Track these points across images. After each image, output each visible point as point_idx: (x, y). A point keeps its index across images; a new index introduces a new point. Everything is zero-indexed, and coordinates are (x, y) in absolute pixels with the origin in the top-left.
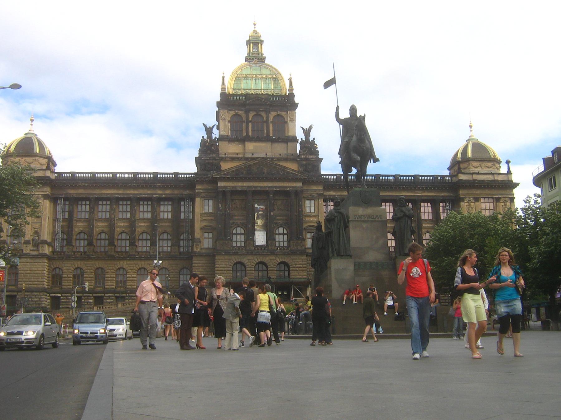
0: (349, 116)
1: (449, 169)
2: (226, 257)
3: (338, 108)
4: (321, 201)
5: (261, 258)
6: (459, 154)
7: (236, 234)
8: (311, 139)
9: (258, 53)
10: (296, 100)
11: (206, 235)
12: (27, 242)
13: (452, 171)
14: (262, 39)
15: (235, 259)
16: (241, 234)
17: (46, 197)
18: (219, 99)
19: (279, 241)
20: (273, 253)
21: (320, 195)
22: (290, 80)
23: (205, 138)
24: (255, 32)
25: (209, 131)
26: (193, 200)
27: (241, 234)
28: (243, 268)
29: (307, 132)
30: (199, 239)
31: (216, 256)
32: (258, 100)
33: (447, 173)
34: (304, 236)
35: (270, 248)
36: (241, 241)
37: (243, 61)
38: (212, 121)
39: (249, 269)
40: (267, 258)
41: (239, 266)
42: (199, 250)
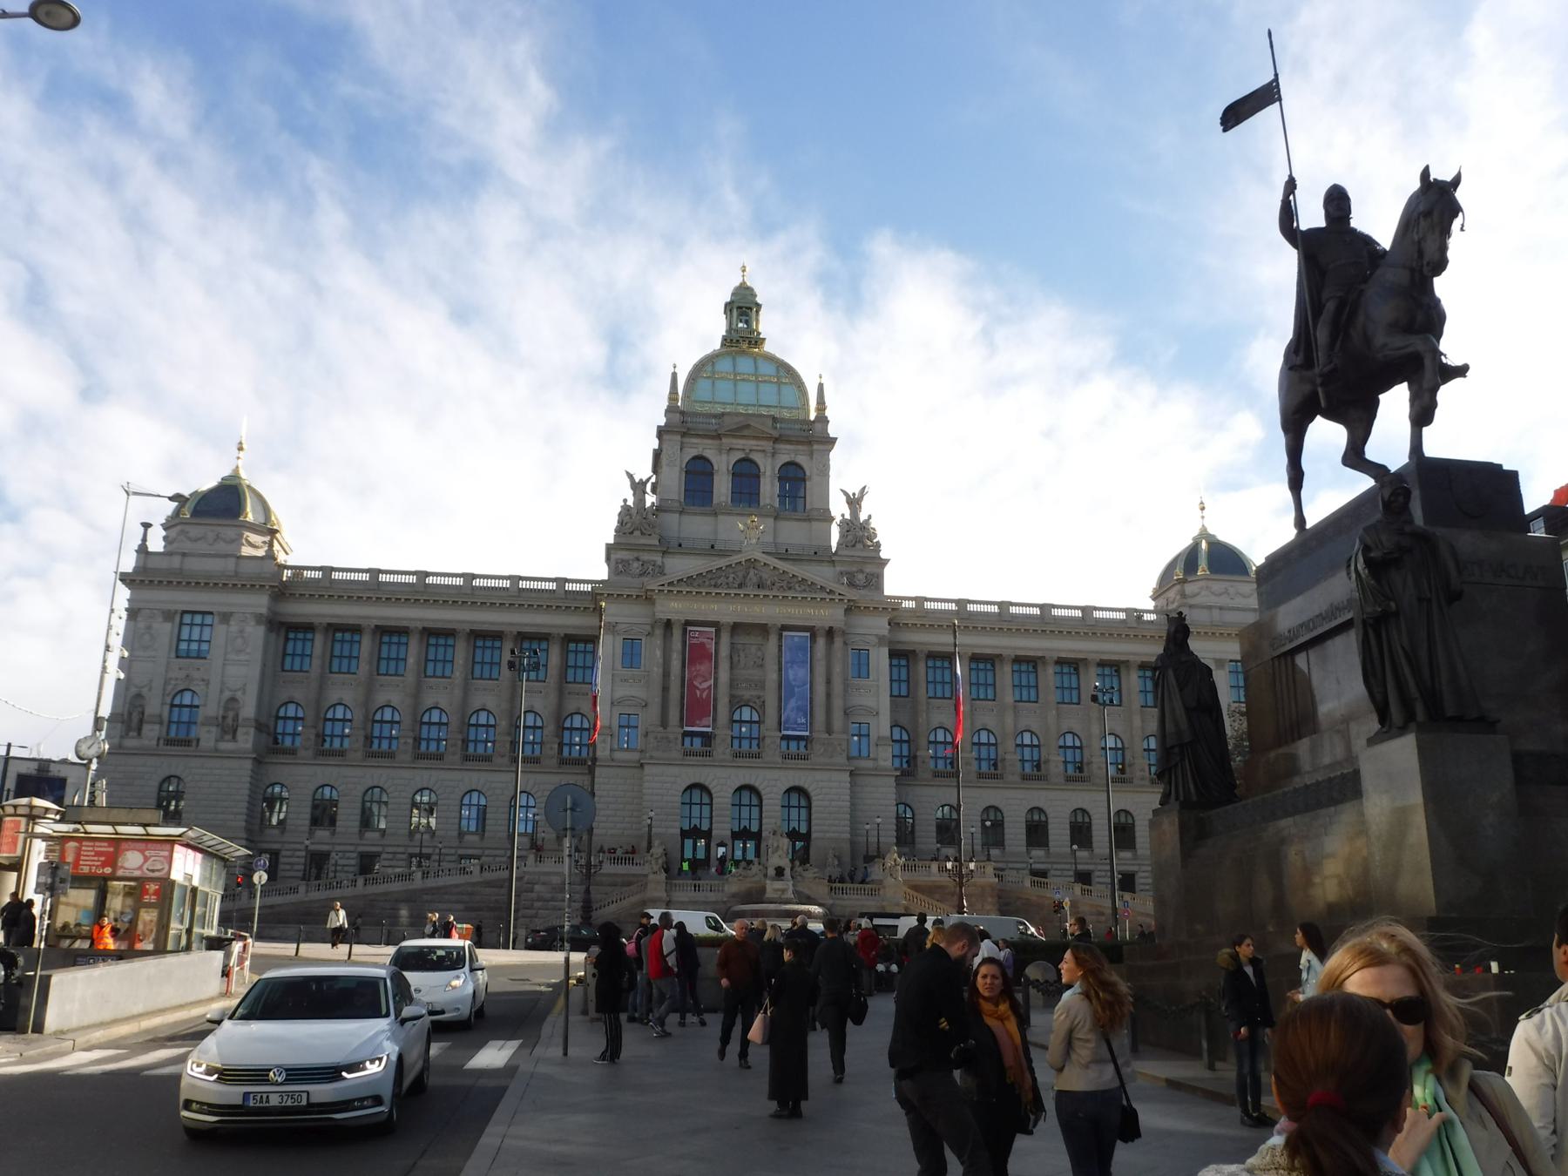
0: (1322, 224)
1: (1154, 598)
3: (1291, 185)
4: (885, 651)
6: (1180, 565)
8: (863, 517)
9: (752, 332)
10: (832, 432)
12: (208, 722)
13: (1162, 601)
14: (759, 300)
17: (259, 618)
18: (662, 421)
21: (881, 640)
22: (821, 387)
23: (630, 503)
24: (744, 283)
25: (638, 487)
26: (593, 640)
28: (706, 800)
29: (854, 502)
32: (748, 426)
33: (1151, 605)
37: (717, 346)
38: (644, 471)
41: (696, 795)
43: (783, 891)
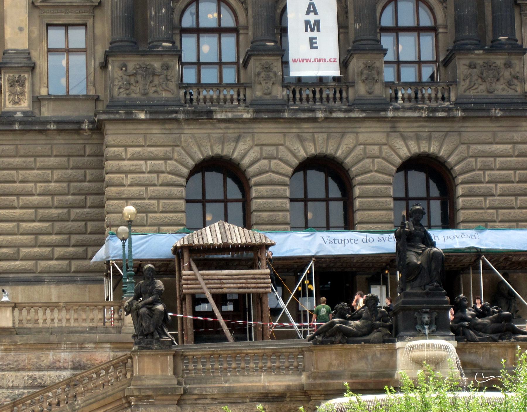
2: (156, 131)
5: (320, 138)
7: (198, 31)
11: (56, 37)
15: (201, 142)
16: (219, 31)
19: (398, 63)
20: (375, 110)
27: (219, 31)
28: (234, 191)
30: (27, 54)
31: (109, 128)
34: (518, 36)
35: (362, 89)
36: (220, 64)
39: (264, 190)
40: (349, 140)
41: (214, 179)
42: (25, 104)
43: (437, 363)
